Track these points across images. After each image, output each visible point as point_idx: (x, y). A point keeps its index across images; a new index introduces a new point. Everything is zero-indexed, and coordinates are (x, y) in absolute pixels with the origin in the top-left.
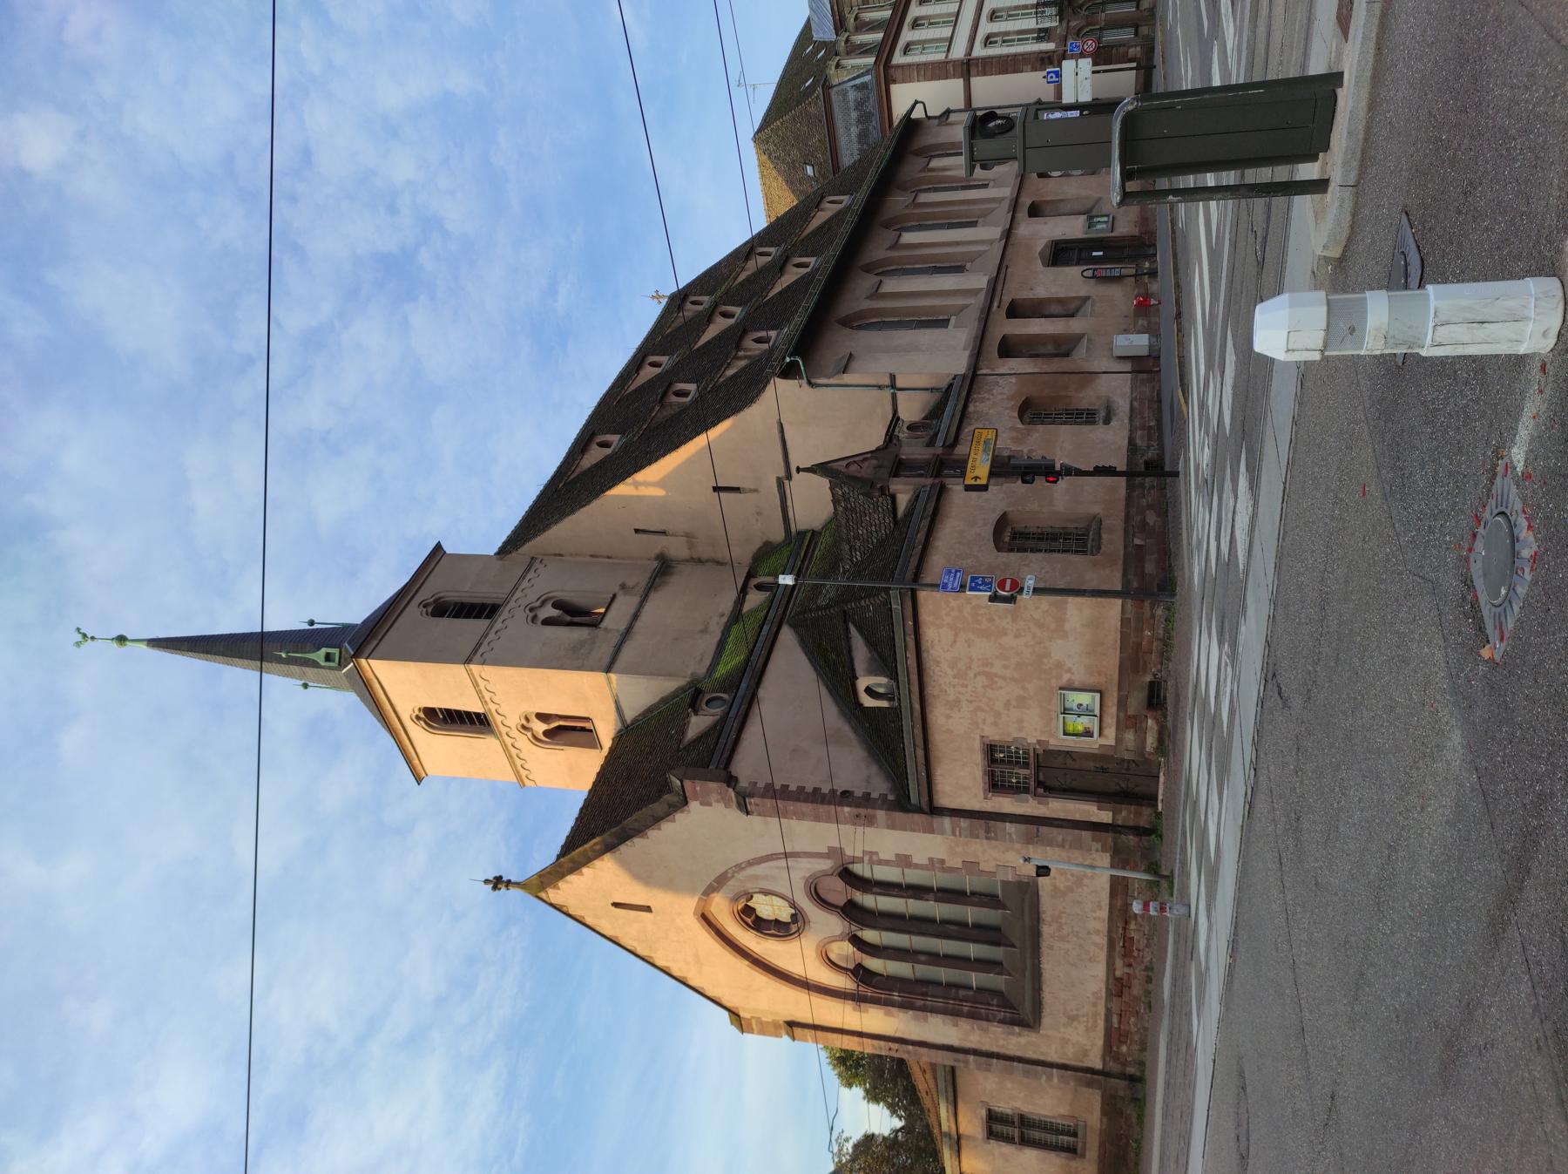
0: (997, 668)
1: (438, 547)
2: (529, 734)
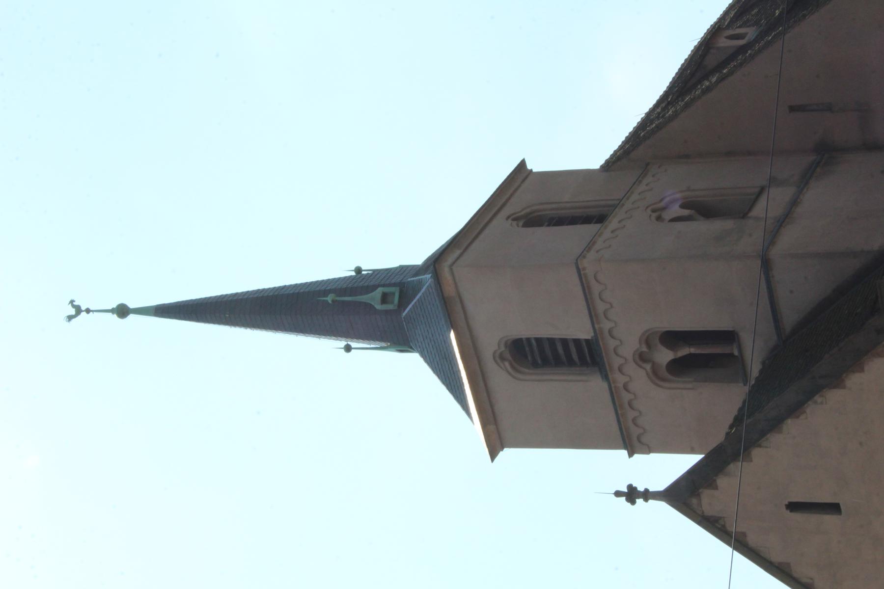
1: (522, 164)
2: (648, 367)
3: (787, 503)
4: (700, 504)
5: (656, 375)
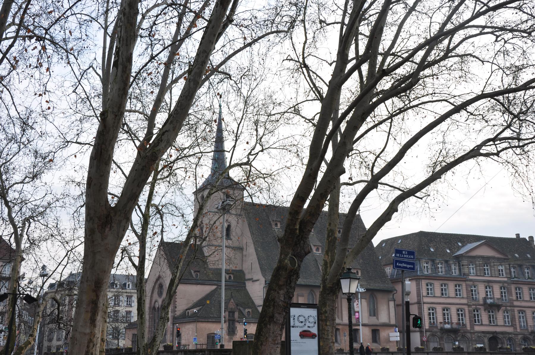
0: (189, 336)
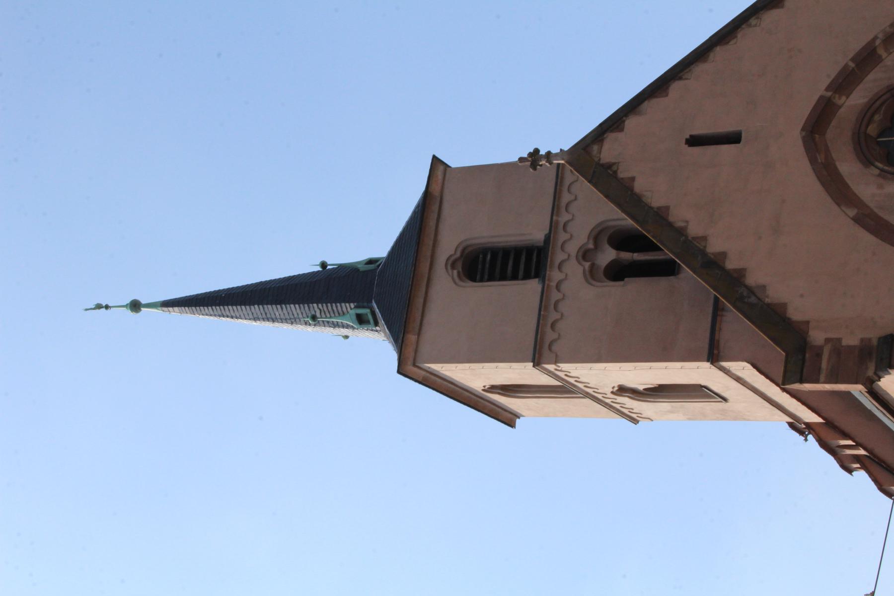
3: (688, 137)
4: (600, 152)
5: (592, 275)
